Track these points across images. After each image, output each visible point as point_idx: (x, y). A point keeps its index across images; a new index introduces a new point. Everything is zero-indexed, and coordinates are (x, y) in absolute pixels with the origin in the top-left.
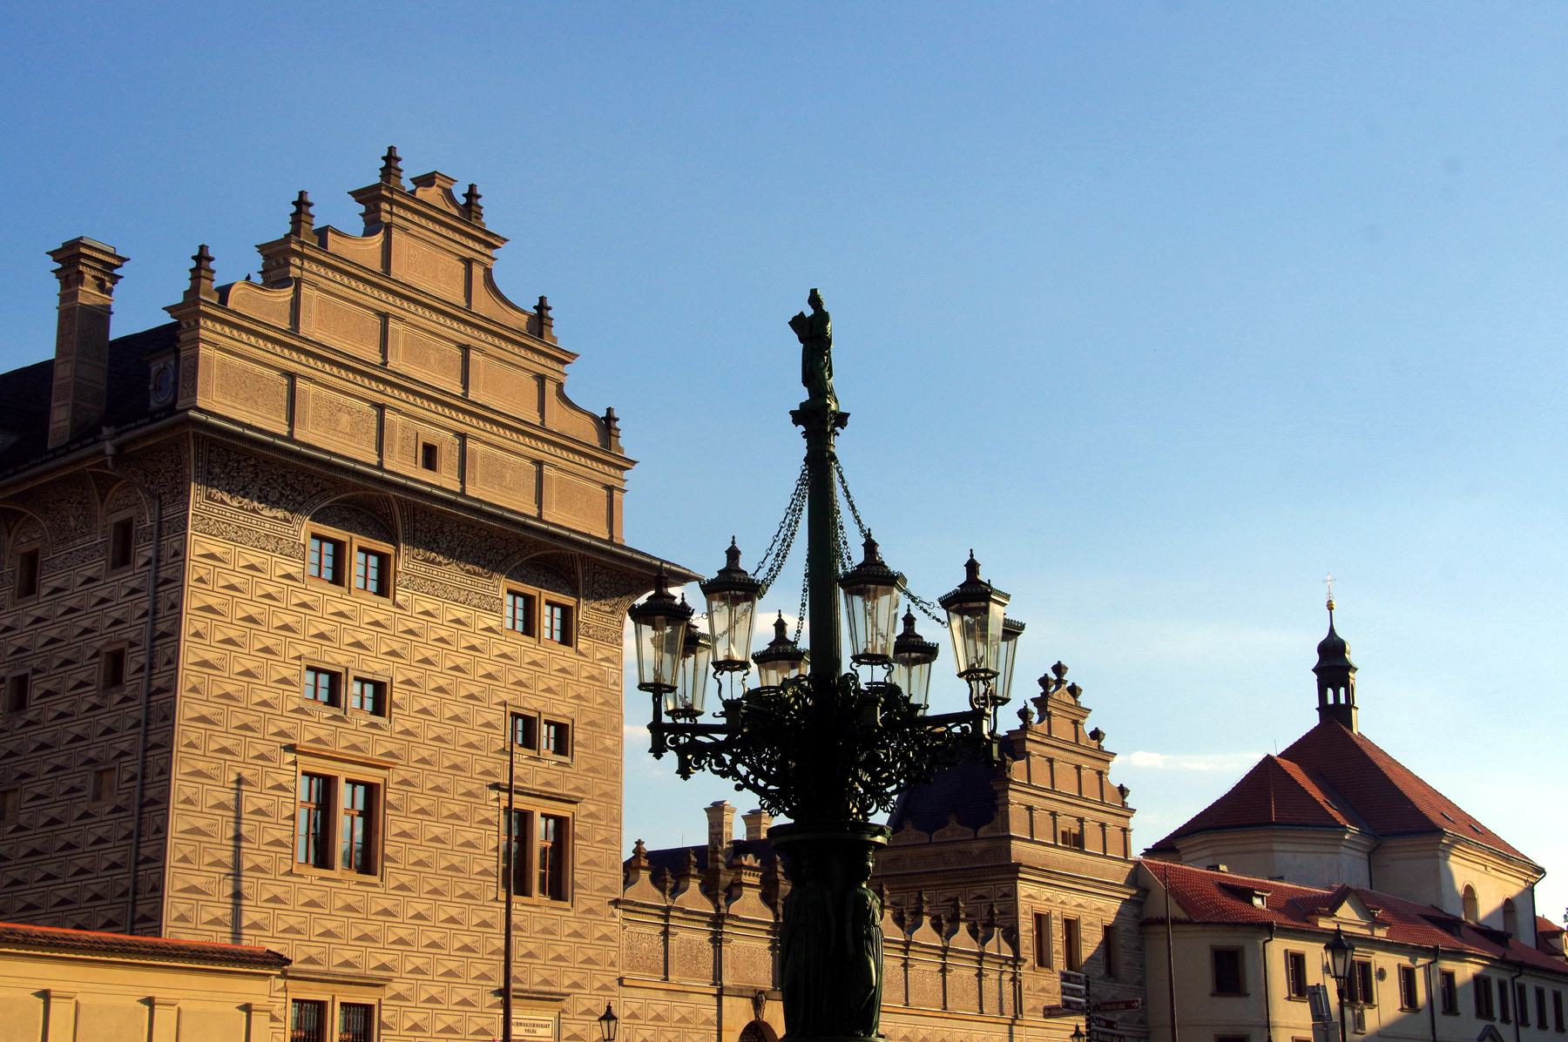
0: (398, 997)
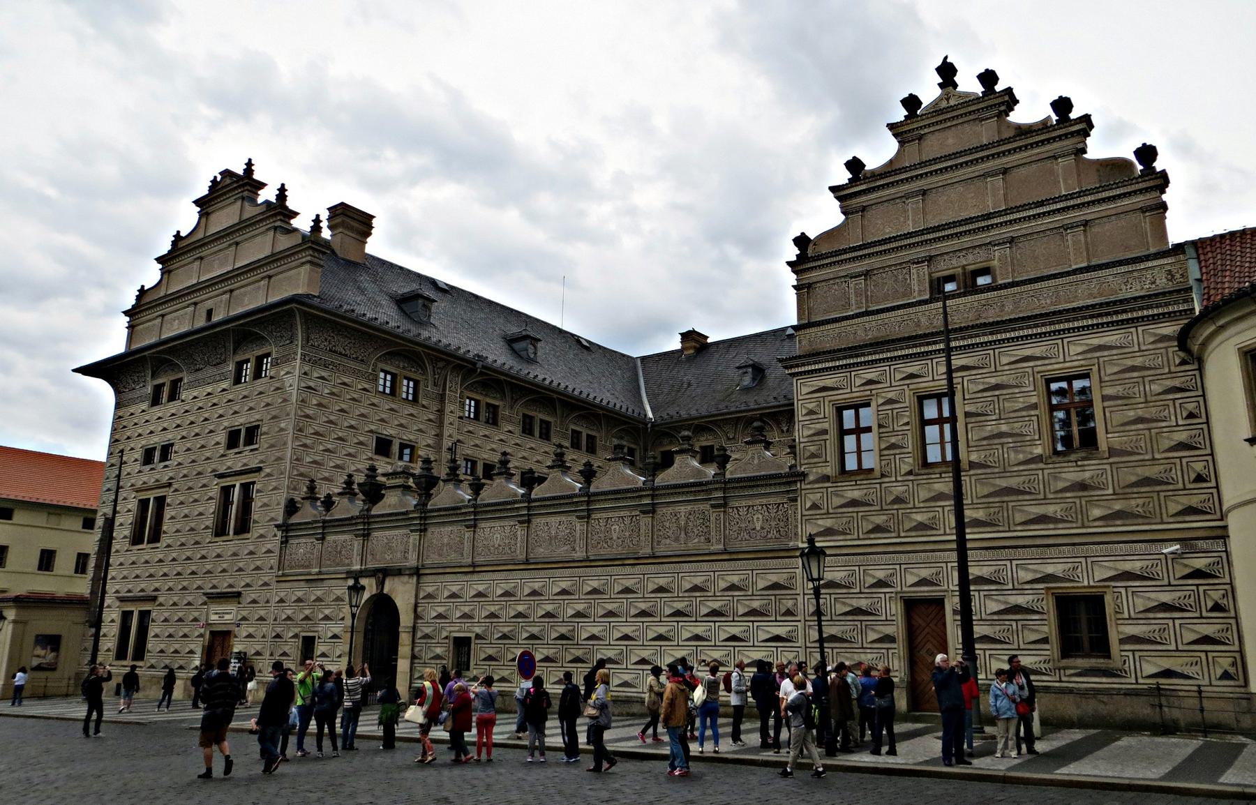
0: (161, 605)
